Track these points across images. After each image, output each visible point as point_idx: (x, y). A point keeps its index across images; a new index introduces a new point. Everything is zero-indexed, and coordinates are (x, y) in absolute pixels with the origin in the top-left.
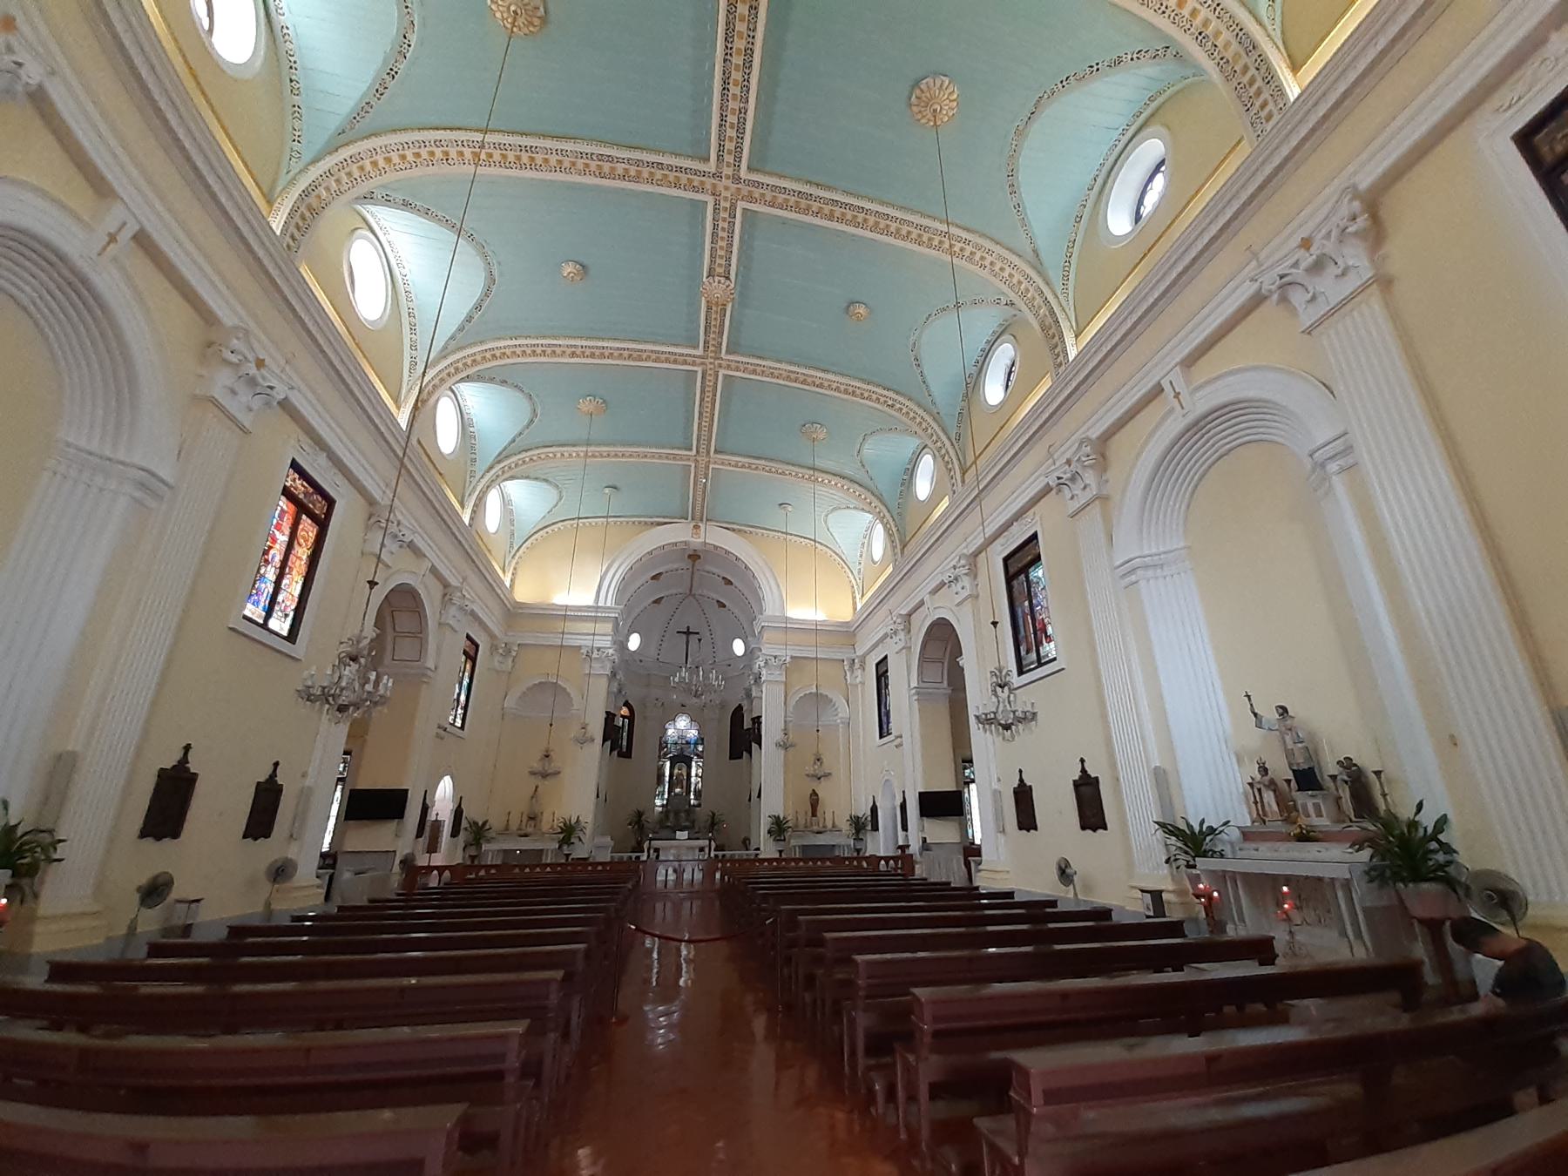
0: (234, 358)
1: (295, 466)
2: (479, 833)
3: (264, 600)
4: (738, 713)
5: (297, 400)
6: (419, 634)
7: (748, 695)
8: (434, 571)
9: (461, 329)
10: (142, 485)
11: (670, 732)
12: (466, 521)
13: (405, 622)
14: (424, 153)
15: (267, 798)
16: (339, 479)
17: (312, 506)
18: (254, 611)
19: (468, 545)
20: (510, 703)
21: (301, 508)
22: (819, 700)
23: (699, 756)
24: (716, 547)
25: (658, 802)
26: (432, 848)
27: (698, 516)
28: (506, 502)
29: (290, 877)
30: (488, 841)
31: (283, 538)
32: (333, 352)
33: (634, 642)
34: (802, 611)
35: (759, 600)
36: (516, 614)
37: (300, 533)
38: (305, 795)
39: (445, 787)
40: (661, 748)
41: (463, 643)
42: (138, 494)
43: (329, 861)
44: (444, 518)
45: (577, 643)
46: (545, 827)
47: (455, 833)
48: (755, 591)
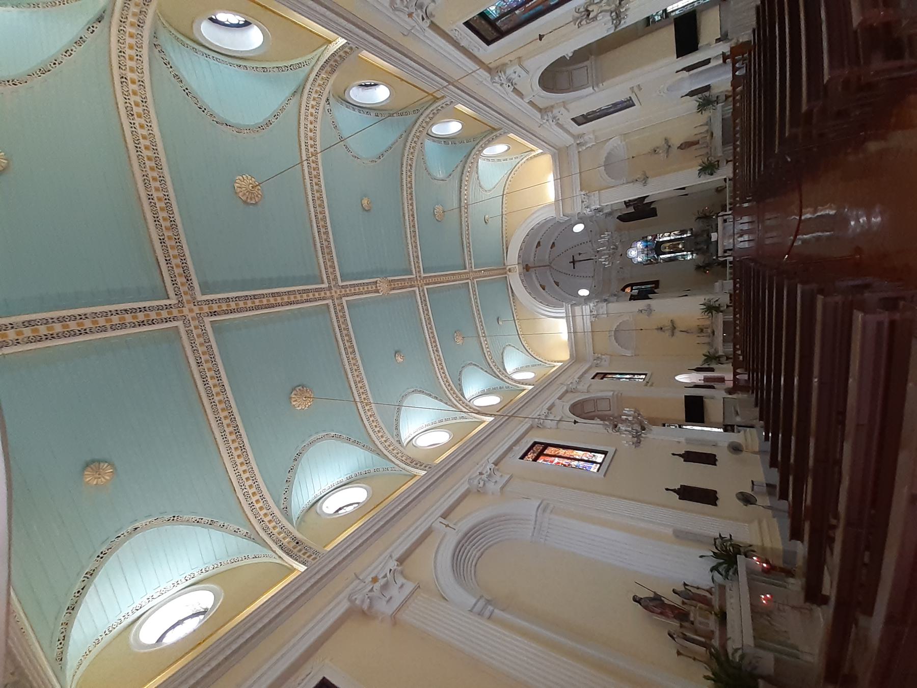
0: (481, 485)
1: (522, 458)
2: (712, 359)
3: (589, 465)
4: (624, 218)
5: (493, 460)
6: (595, 401)
7: (610, 214)
8: (560, 398)
9: (441, 401)
10: (544, 511)
11: (640, 260)
12: (531, 387)
13: (589, 408)
14: (374, 424)
15: (689, 457)
16: (524, 441)
17: (539, 450)
18: (594, 468)
19: (543, 386)
20: (629, 353)
21: (541, 454)
22: (609, 165)
23: (655, 237)
24: (519, 256)
25: (689, 257)
26: (722, 380)
27: (504, 270)
28: (518, 371)
29: (740, 445)
30: (716, 351)
31: (557, 460)
32: (468, 450)
33: (584, 292)
34: (550, 193)
35: (547, 222)
36: (576, 357)
37: (553, 453)
38: (689, 441)
39: (682, 378)
40: (651, 263)
41: (597, 380)
42: (549, 511)
43: (728, 428)
44: (532, 398)
45: (589, 324)
46: (708, 323)
47: (712, 370)
48: (541, 226)
